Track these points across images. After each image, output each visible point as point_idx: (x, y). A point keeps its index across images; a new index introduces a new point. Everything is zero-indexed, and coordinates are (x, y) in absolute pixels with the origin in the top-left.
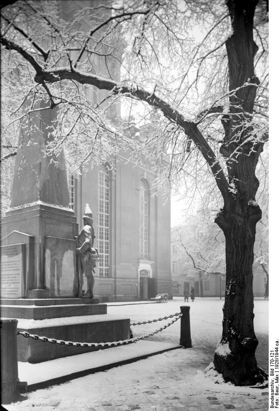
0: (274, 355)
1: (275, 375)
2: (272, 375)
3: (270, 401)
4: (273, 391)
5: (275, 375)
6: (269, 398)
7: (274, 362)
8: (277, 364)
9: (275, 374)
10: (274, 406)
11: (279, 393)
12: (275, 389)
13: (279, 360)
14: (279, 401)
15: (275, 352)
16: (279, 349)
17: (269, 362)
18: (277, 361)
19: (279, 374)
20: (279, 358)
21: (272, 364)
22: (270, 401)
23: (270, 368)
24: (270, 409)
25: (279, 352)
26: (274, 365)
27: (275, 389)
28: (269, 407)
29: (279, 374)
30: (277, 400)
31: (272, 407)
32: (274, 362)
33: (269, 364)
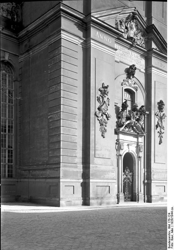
0: (171, 216)
2: (169, 228)
3: (168, 244)
4: (170, 238)
6: (168, 242)
7: (170, 220)
8: (172, 221)
10: (170, 247)
12: (171, 237)
14: (173, 244)
15: (171, 214)
16: (173, 213)
17: (168, 220)
18: (172, 219)
19: (173, 227)
20: (173, 217)
21: (169, 222)
23: (168, 224)
25: (173, 214)
26: (170, 222)
27: (171, 237)
29: (173, 227)
30: (172, 243)
31: (169, 248)
32: (170, 220)
33: (168, 222)
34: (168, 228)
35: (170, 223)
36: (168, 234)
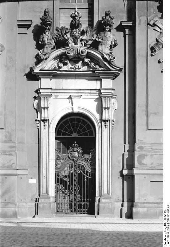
0: (167, 213)
1: (167, 226)
2: (165, 225)
3: (164, 241)
4: (166, 235)
5: (167, 226)
7: (166, 218)
8: (168, 219)
9: (167, 225)
10: (166, 244)
11: (169, 236)
12: (167, 234)
13: (169, 216)
14: (169, 241)
15: (167, 212)
16: (169, 210)
18: (168, 217)
19: (169, 225)
20: (169, 215)
21: (165, 219)
22: (164, 241)
24: (164, 246)
25: (169, 212)
26: (167, 219)
27: (167, 234)
28: (164, 245)
29: (169, 224)
30: (168, 240)
31: (165, 245)
32: (166, 218)
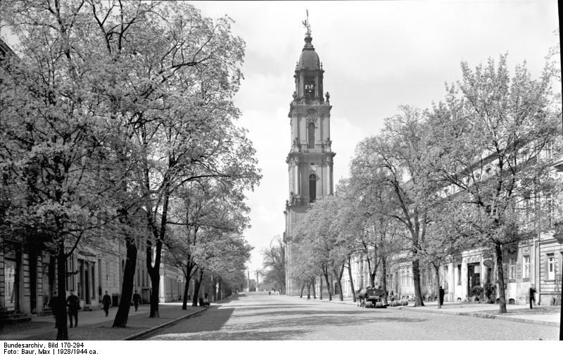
1: (49, 349)
2: (50, 345)
3: (14, 342)
4: (27, 346)
5: (49, 349)
7: (67, 348)
8: (64, 351)
9: (51, 349)
12: (30, 349)
15: (81, 348)
17: (67, 342)
23: (60, 342)
26: (64, 348)
27: (30, 349)
30: (15, 352)
31: (5, 345)
32: (67, 348)
34: (50, 341)
35: (60, 345)
36: (37, 342)
